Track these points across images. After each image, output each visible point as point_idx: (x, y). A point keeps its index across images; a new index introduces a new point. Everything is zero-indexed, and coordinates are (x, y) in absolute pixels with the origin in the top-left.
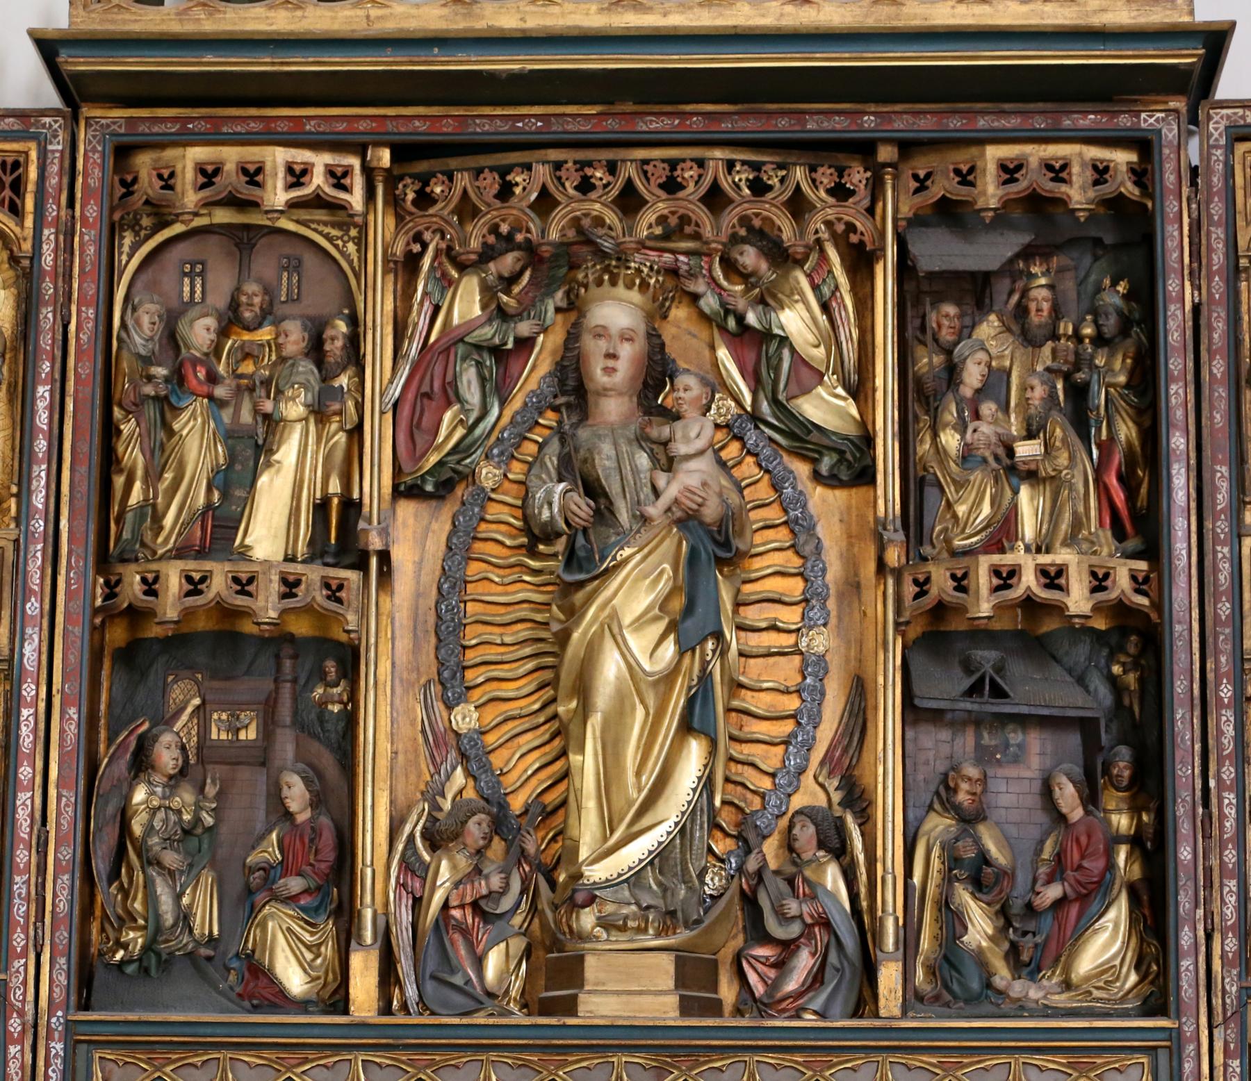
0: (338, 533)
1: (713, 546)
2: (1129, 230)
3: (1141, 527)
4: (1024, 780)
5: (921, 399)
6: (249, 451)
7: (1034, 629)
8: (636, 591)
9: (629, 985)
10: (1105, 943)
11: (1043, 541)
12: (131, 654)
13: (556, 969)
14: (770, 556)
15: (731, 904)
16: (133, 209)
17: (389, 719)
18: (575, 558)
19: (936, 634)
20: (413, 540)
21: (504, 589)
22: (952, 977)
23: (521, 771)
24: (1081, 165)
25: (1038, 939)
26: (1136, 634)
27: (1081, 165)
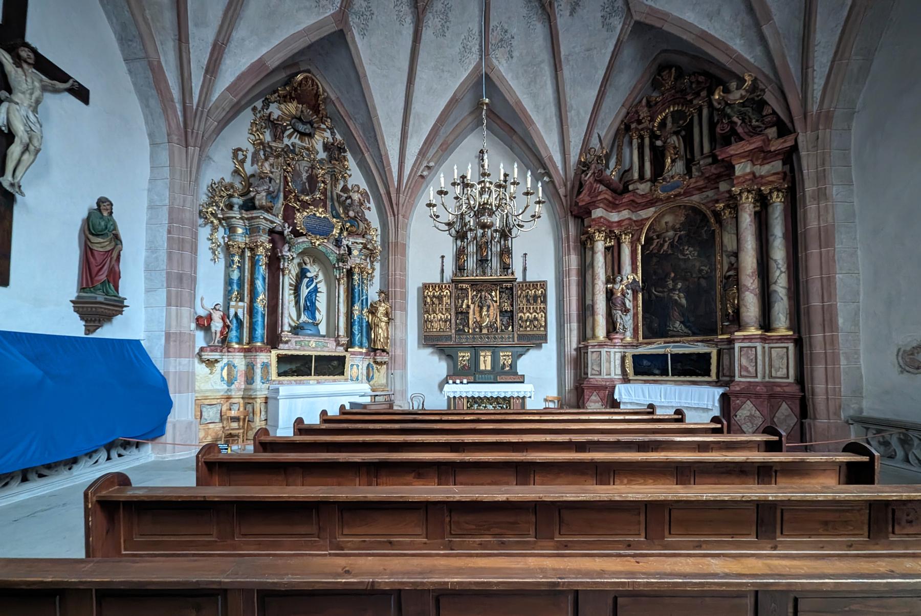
0: (468, 306)
1: (489, 307)
2: (512, 289)
3: (512, 305)
4: (505, 320)
5: (500, 298)
6: (463, 302)
7: (506, 311)
8: (485, 309)
9: (485, 331)
10: (510, 328)
11: (507, 307)
12: (457, 313)
13: (481, 331)
14: (492, 308)
15: (491, 326)
16: (456, 288)
17: (471, 316)
18: (481, 308)
19: (501, 312)
20: (472, 306)
21: (477, 309)
22: (502, 331)
23: (478, 319)
24: (509, 285)
25: (507, 328)
26: (512, 312)
27: (509, 285)
